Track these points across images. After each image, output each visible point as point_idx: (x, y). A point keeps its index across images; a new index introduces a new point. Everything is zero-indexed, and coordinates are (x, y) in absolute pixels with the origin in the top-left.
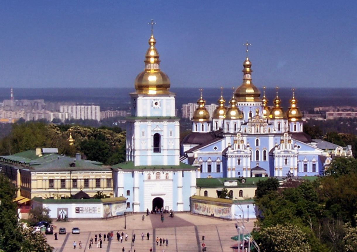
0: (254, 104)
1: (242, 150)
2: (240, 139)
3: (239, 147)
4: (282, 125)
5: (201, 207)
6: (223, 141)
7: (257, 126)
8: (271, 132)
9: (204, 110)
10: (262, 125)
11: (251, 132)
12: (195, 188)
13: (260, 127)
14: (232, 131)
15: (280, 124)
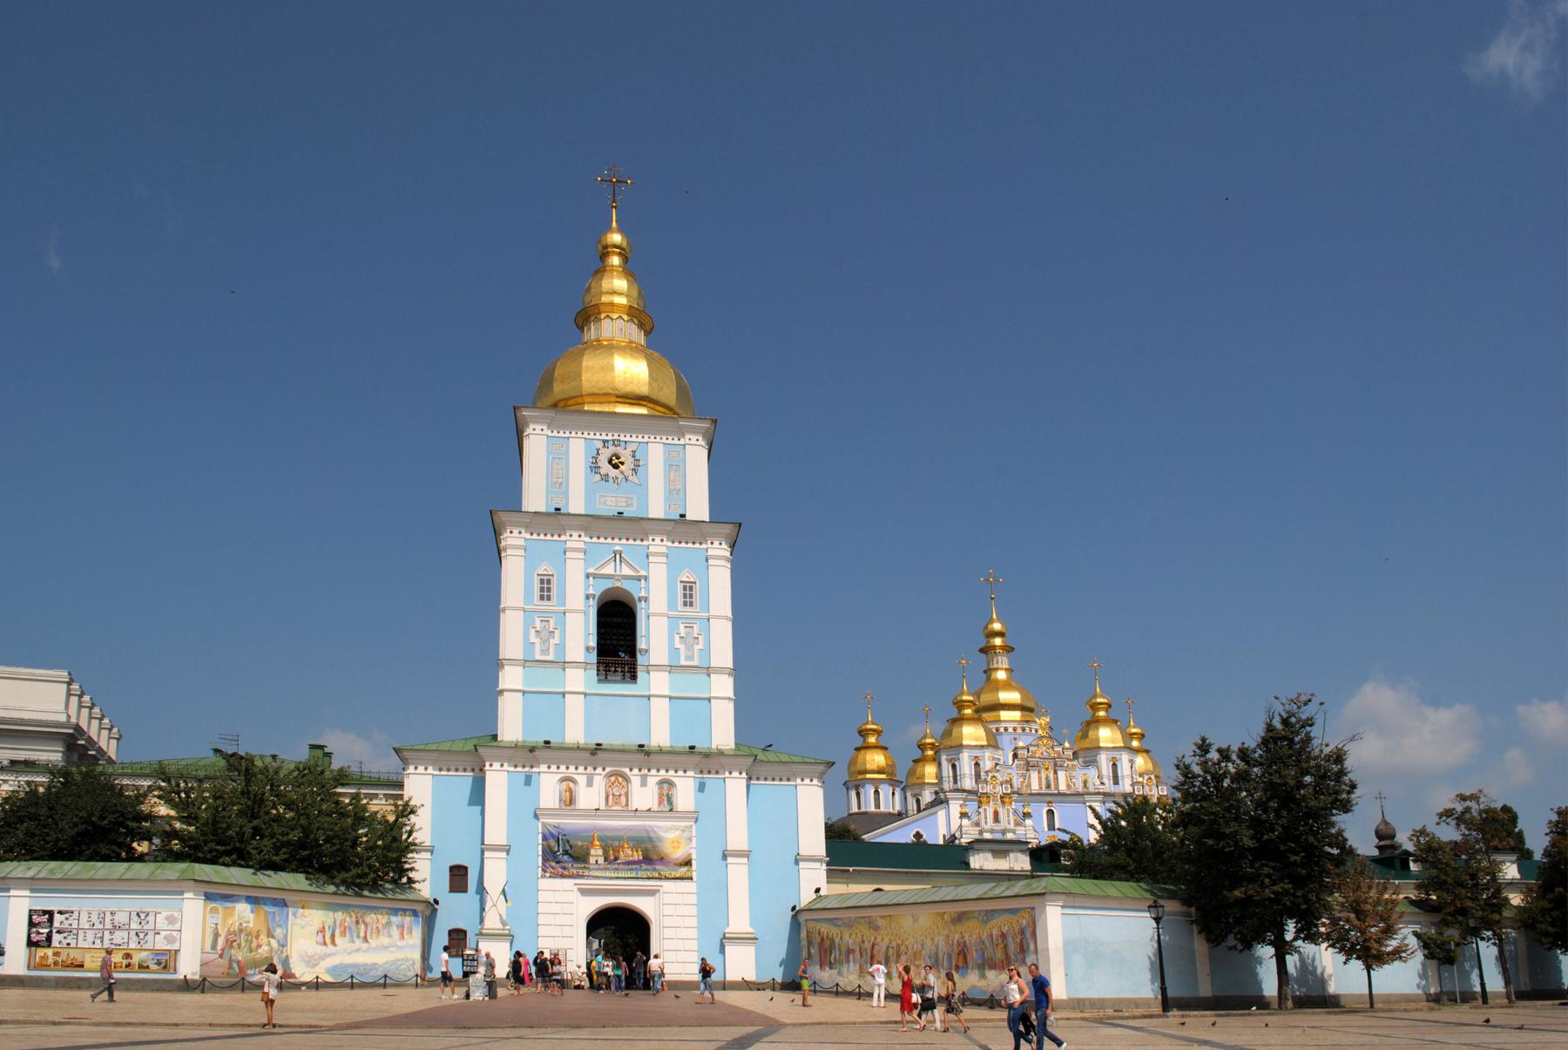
0: (1024, 730)
1: (1008, 827)
2: (1000, 790)
3: (996, 819)
4: (1124, 769)
5: (850, 951)
6: (941, 814)
7: (1047, 769)
8: (1091, 790)
9: (879, 751)
10: (1061, 766)
11: (1029, 785)
12: (817, 865)
13: (1055, 772)
14: (968, 783)
15: (1117, 763)
